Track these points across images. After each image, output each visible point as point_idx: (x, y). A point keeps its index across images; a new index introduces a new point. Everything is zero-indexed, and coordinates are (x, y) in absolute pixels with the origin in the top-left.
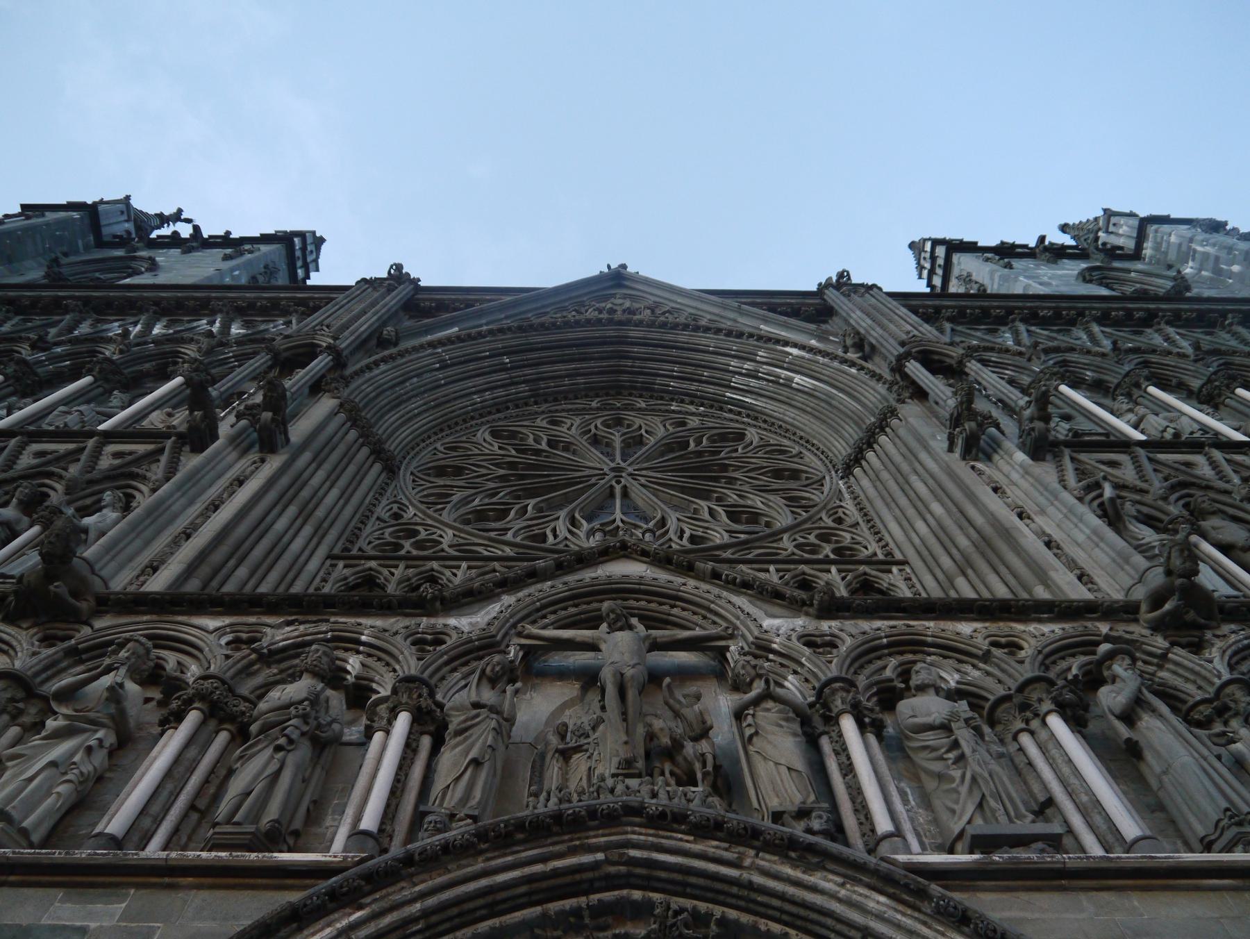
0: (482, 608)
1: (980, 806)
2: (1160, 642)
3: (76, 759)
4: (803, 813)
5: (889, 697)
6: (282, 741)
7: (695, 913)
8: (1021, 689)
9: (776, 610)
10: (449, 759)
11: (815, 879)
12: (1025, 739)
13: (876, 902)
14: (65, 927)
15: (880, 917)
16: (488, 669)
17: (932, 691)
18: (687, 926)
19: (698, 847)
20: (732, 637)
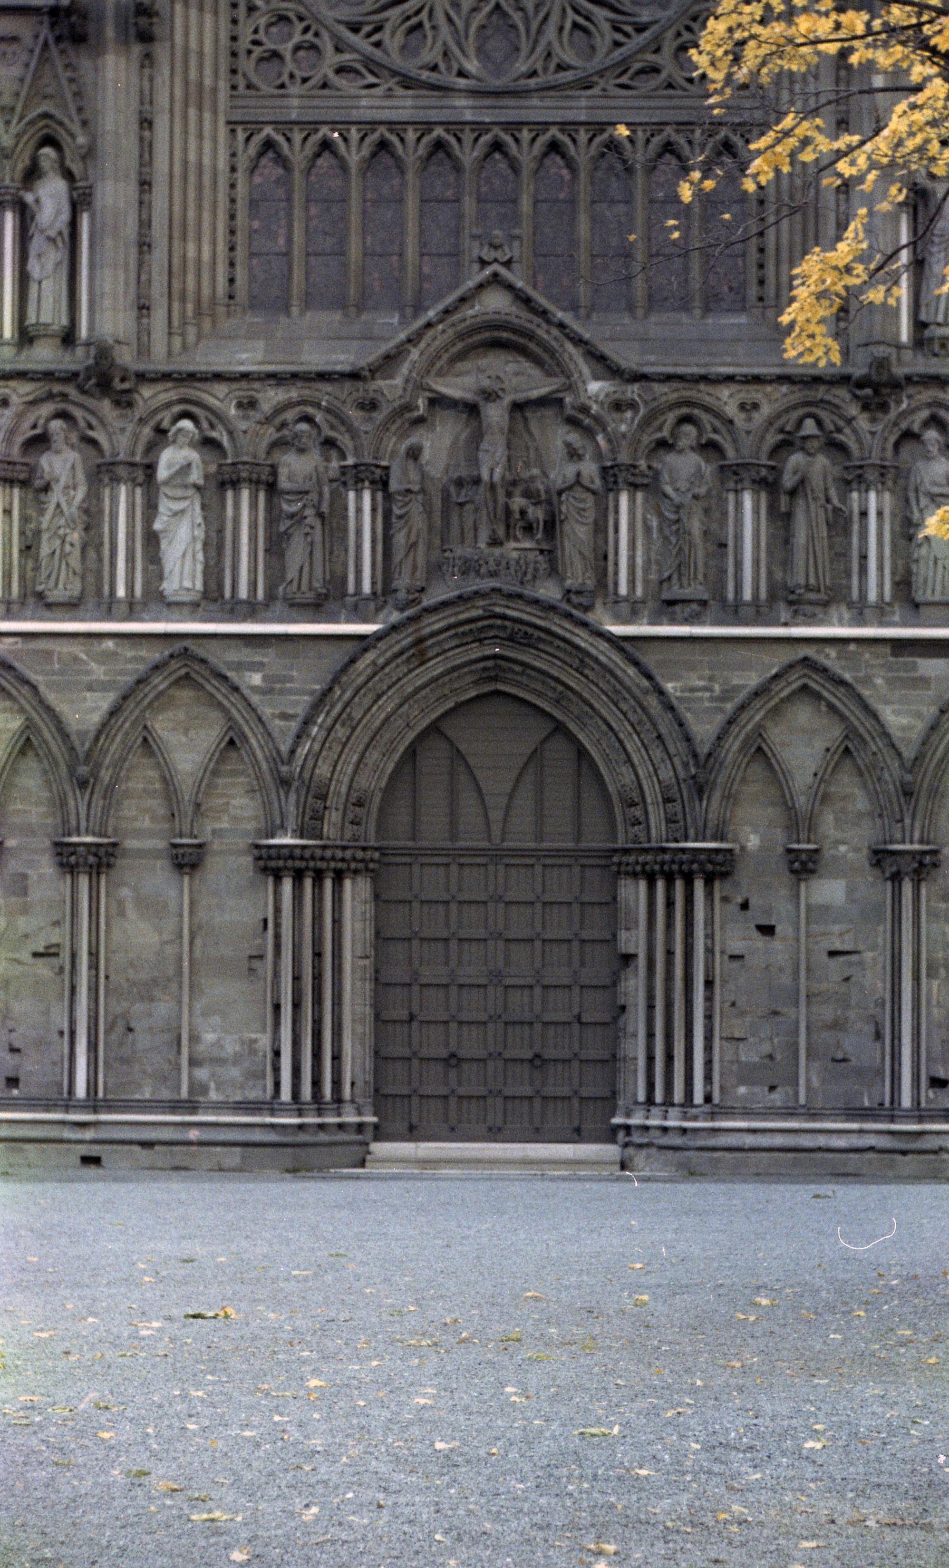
2: (853, 410)
4: (579, 593)
5: (663, 445)
6: (307, 529)
9: (599, 368)
12: (731, 497)
13: (604, 645)
17: (688, 451)
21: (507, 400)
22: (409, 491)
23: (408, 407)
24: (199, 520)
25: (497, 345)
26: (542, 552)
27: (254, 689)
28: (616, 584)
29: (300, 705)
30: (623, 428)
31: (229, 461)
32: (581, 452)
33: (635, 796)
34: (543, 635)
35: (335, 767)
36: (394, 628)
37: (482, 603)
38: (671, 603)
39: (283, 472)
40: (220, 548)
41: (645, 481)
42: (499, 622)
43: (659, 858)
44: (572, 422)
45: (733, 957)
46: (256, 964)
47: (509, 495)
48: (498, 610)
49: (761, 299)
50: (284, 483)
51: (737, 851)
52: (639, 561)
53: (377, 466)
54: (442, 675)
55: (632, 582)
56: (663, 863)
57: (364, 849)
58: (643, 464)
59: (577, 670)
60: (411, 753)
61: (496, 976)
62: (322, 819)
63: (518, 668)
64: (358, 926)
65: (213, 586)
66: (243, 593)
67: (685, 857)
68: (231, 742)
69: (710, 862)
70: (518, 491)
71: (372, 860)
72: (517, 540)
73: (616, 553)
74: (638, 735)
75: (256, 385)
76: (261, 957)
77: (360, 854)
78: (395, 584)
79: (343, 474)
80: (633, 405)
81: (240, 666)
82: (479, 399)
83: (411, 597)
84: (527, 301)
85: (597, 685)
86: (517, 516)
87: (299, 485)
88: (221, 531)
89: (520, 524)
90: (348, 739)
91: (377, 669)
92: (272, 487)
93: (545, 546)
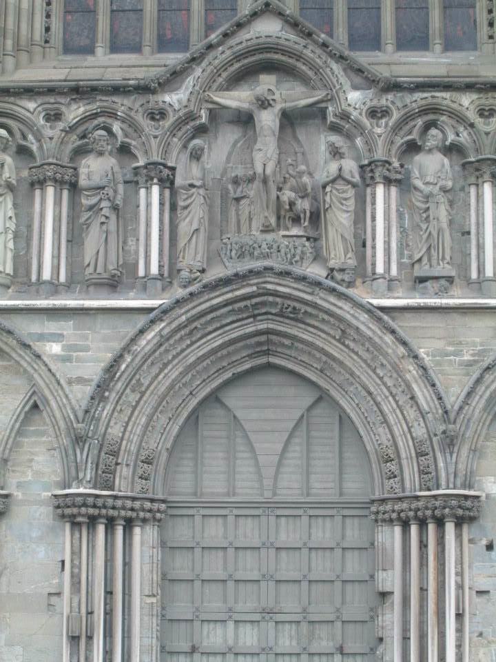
0: (183, 81)
1: (429, 248)
3: (8, 226)
4: (342, 270)
5: (412, 148)
6: (103, 219)
7: (294, 308)
8: (478, 161)
9: (358, 80)
10: (184, 227)
11: (340, 304)
12: (473, 190)
13: (364, 317)
14: (54, 334)
15: (363, 323)
16: (194, 152)
17: (435, 151)
18: (291, 312)
19: (295, 285)
20: (330, 100)
21: (278, 107)
22: (192, 186)
23: (190, 117)
24: (11, 213)
25: (269, 67)
26: (308, 239)
27: (57, 358)
28: (374, 265)
29: (93, 370)
30: (379, 131)
31: (38, 164)
32: (342, 151)
33: (391, 452)
34: (309, 310)
35: (126, 428)
36: (179, 303)
37: (256, 281)
38: (422, 280)
39: (83, 171)
40: (29, 240)
41: (399, 177)
42: (271, 299)
43: (413, 506)
44: (334, 128)
45: (480, 593)
46: (54, 600)
47: (280, 189)
48: (269, 286)
49: (491, 37)
50: (83, 182)
51: (483, 498)
52: (394, 245)
53: (165, 166)
54: (221, 347)
55: (388, 263)
56: (418, 510)
57: (152, 501)
58: (396, 164)
59: (339, 341)
60: (194, 419)
61: (267, 612)
62: (114, 473)
63: (287, 342)
64: (147, 568)
65: (22, 271)
66: (47, 275)
67: (437, 503)
68: (35, 406)
69: (460, 507)
70: (288, 185)
71: (159, 511)
72: (287, 229)
73: (374, 239)
74: (394, 397)
75: (62, 100)
76: (59, 594)
77: (148, 505)
78: (179, 266)
79: (136, 174)
80: (386, 113)
81: (42, 337)
82: (253, 108)
83: (193, 276)
84: (295, 25)
85: (357, 354)
86: (288, 207)
87: (96, 180)
88: (30, 227)
89: (288, 215)
90: (138, 402)
91: (163, 340)
92: (74, 187)
93: (311, 234)
